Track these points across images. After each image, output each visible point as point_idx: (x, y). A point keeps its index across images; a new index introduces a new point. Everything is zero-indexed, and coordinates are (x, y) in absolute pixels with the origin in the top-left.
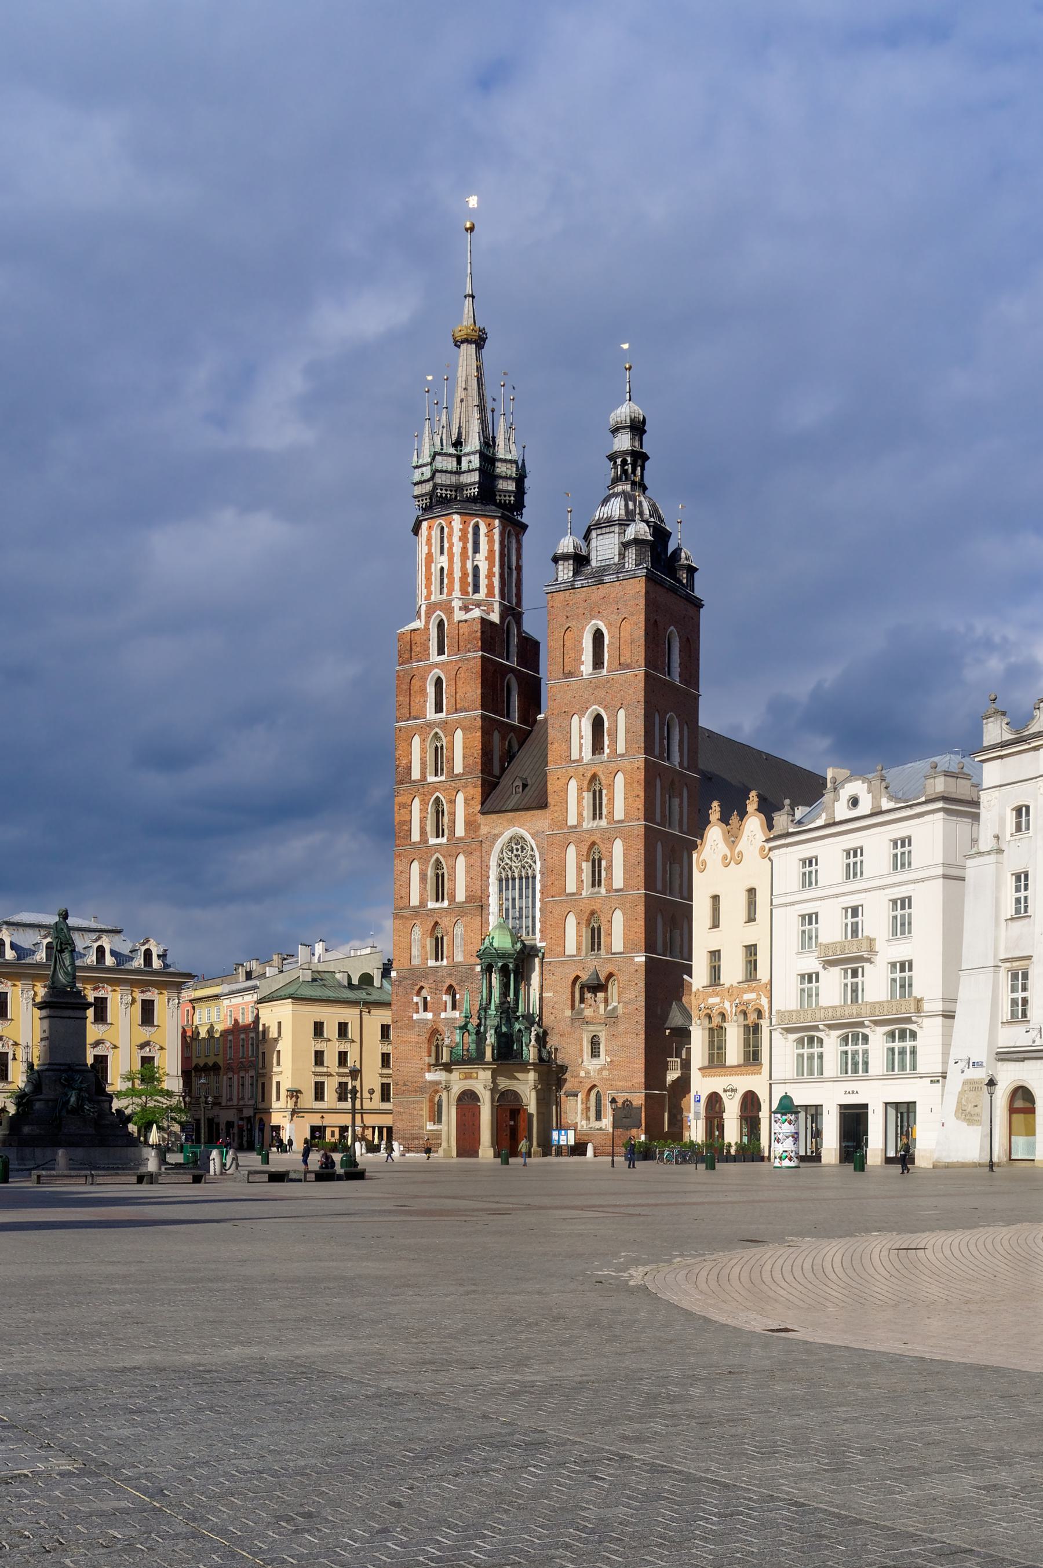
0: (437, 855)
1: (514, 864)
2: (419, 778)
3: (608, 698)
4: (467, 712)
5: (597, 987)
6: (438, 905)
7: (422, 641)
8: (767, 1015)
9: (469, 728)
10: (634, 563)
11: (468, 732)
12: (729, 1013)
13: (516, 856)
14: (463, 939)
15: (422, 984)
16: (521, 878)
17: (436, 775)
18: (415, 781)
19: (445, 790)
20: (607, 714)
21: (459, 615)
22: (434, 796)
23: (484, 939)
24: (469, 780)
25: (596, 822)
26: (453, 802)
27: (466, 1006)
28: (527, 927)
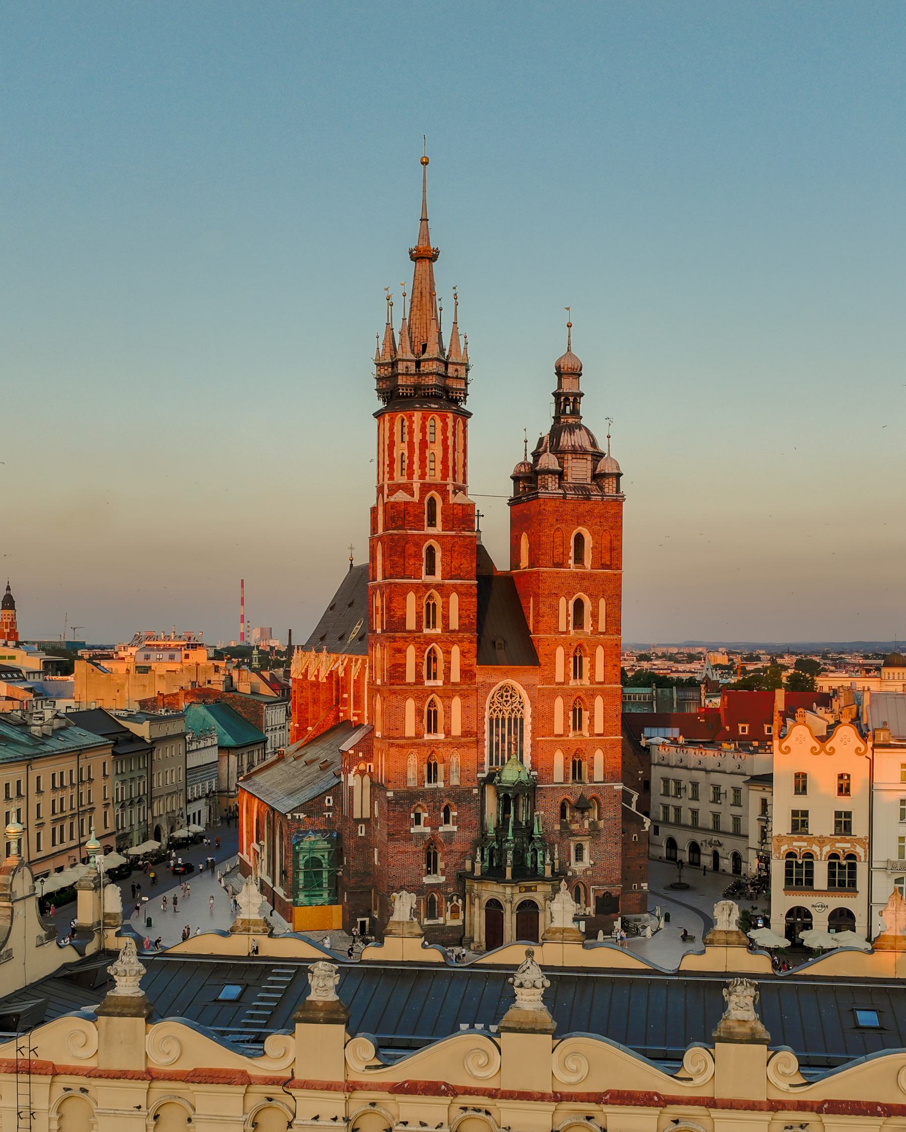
0: (434, 695)
1: (504, 708)
5: (582, 806)
6: (432, 737)
7: (416, 513)
8: (863, 859)
9: (465, 594)
11: (463, 597)
12: (818, 853)
13: (505, 701)
15: (420, 803)
16: (510, 719)
18: (410, 632)
19: (441, 642)
20: (591, 601)
21: (452, 499)
25: (578, 681)
26: (448, 653)
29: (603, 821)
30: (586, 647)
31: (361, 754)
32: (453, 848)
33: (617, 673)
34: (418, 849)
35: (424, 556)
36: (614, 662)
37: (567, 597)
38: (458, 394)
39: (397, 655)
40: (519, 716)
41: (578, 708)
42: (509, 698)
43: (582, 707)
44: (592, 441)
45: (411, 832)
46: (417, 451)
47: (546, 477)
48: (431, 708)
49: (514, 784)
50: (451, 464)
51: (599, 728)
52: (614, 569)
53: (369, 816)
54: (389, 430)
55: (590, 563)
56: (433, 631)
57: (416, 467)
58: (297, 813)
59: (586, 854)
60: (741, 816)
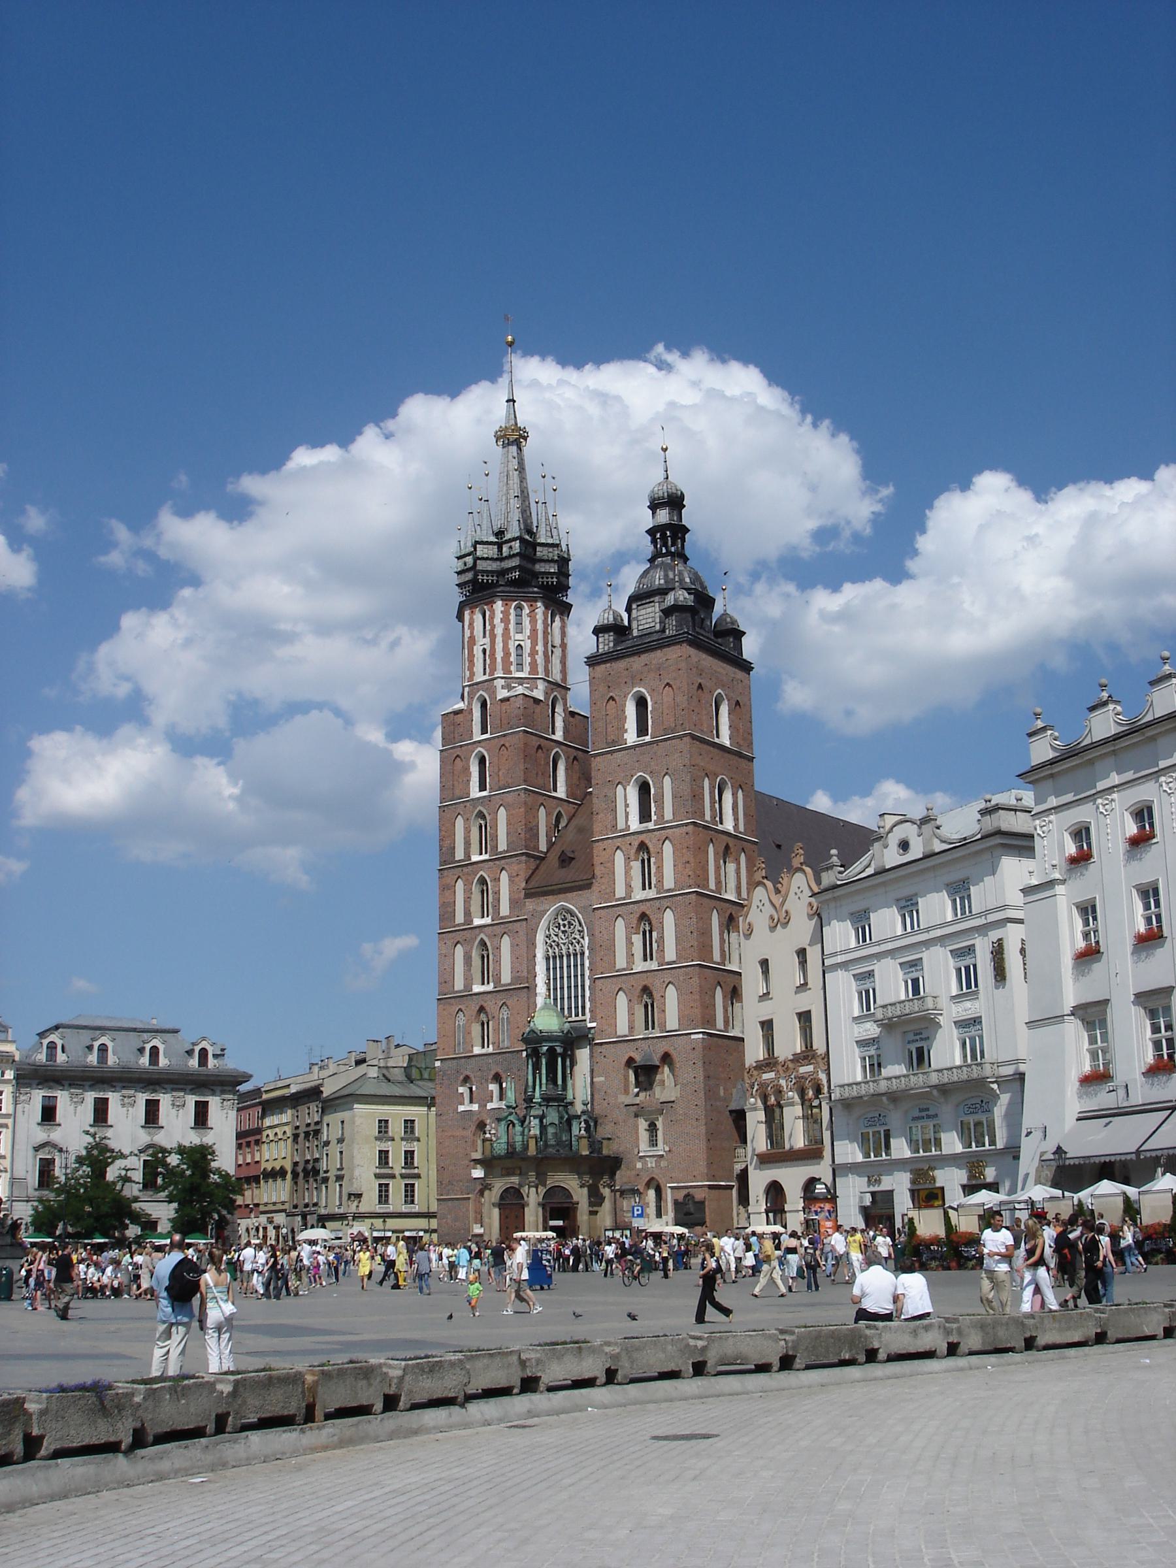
0: (482, 936)
2: (463, 858)
8: (825, 1090)
10: (674, 628)
12: (785, 1089)
14: (508, 1023)
15: (468, 1073)
16: (569, 956)
18: (459, 861)
21: (502, 694)
22: (478, 876)
23: (529, 1022)
27: (511, 1095)
28: (577, 1007)
29: (678, 1087)
34: (464, 1133)
36: (686, 859)
37: (624, 782)
40: (578, 948)
42: (567, 928)
44: (671, 575)
50: (499, 655)
51: (670, 954)
56: (485, 857)
59: (660, 1133)
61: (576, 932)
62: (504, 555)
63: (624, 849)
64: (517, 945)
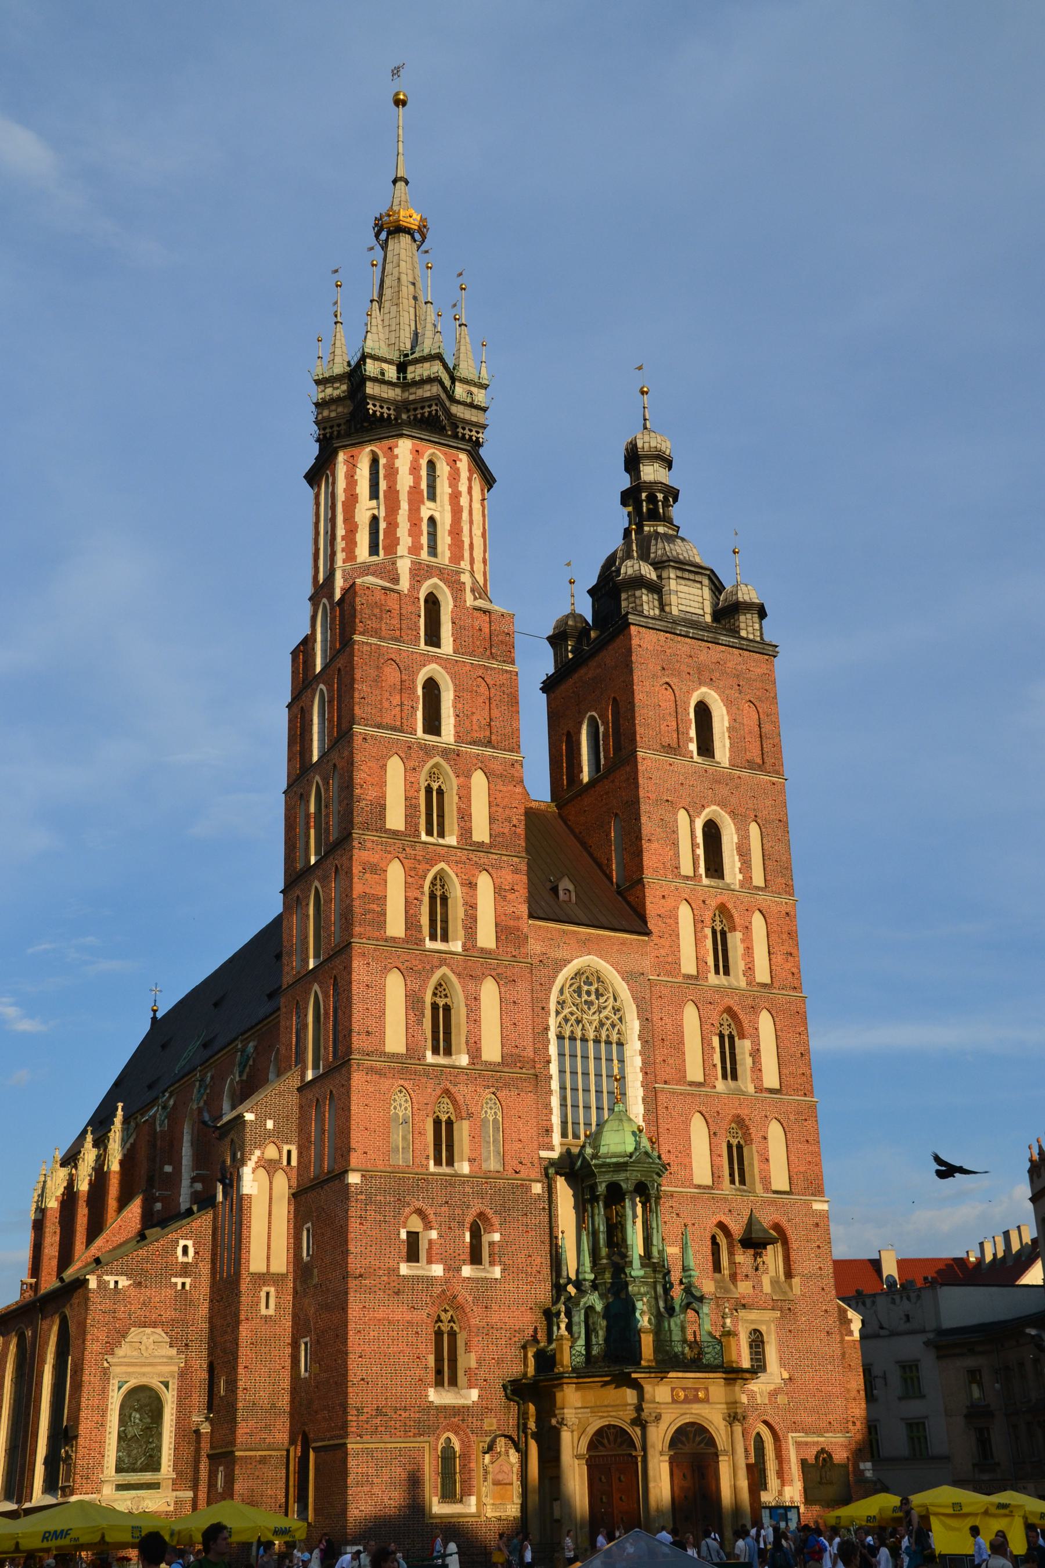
0: (445, 970)
1: (585, 1016)
2: (403, 829)
3: (733, 800)
4: (494, 748)
7: (404, 611)
10: (758, 633)
13: (586, 1002)
14: (496, 1129)
15: (419, 1204)
16: (597, 1041)
17: (429, 833)
18: (395, 833)
19: (457, 862)
24: (505, 858)
29: (796, 1281)
30: (734, 911)
31: (270, 1124)
32: (494, 1318)
33: (794, 970)
35: (420, 692)
36: (786, 948)
37: (691, 810)
38: (474, 433)
39: (367, 875)
41: (726, 1033)
42: (593, 997)
43: (735, 1033)
45: (402, 1273)
46: (404, 506)
47: (638, 593)
48: (438, 1000)
49: (631, 1155)
52: (769, 772)
53: (283, 1270)
54: (346, 477)
55: (728, 755)
56: (441, 841)
57: (403, 531)
58: (112, 1274)
60: (926, 1417)
61: (610, 1007)
62: (457, 397)
63: (693, 906)
64: (514, 1002)
